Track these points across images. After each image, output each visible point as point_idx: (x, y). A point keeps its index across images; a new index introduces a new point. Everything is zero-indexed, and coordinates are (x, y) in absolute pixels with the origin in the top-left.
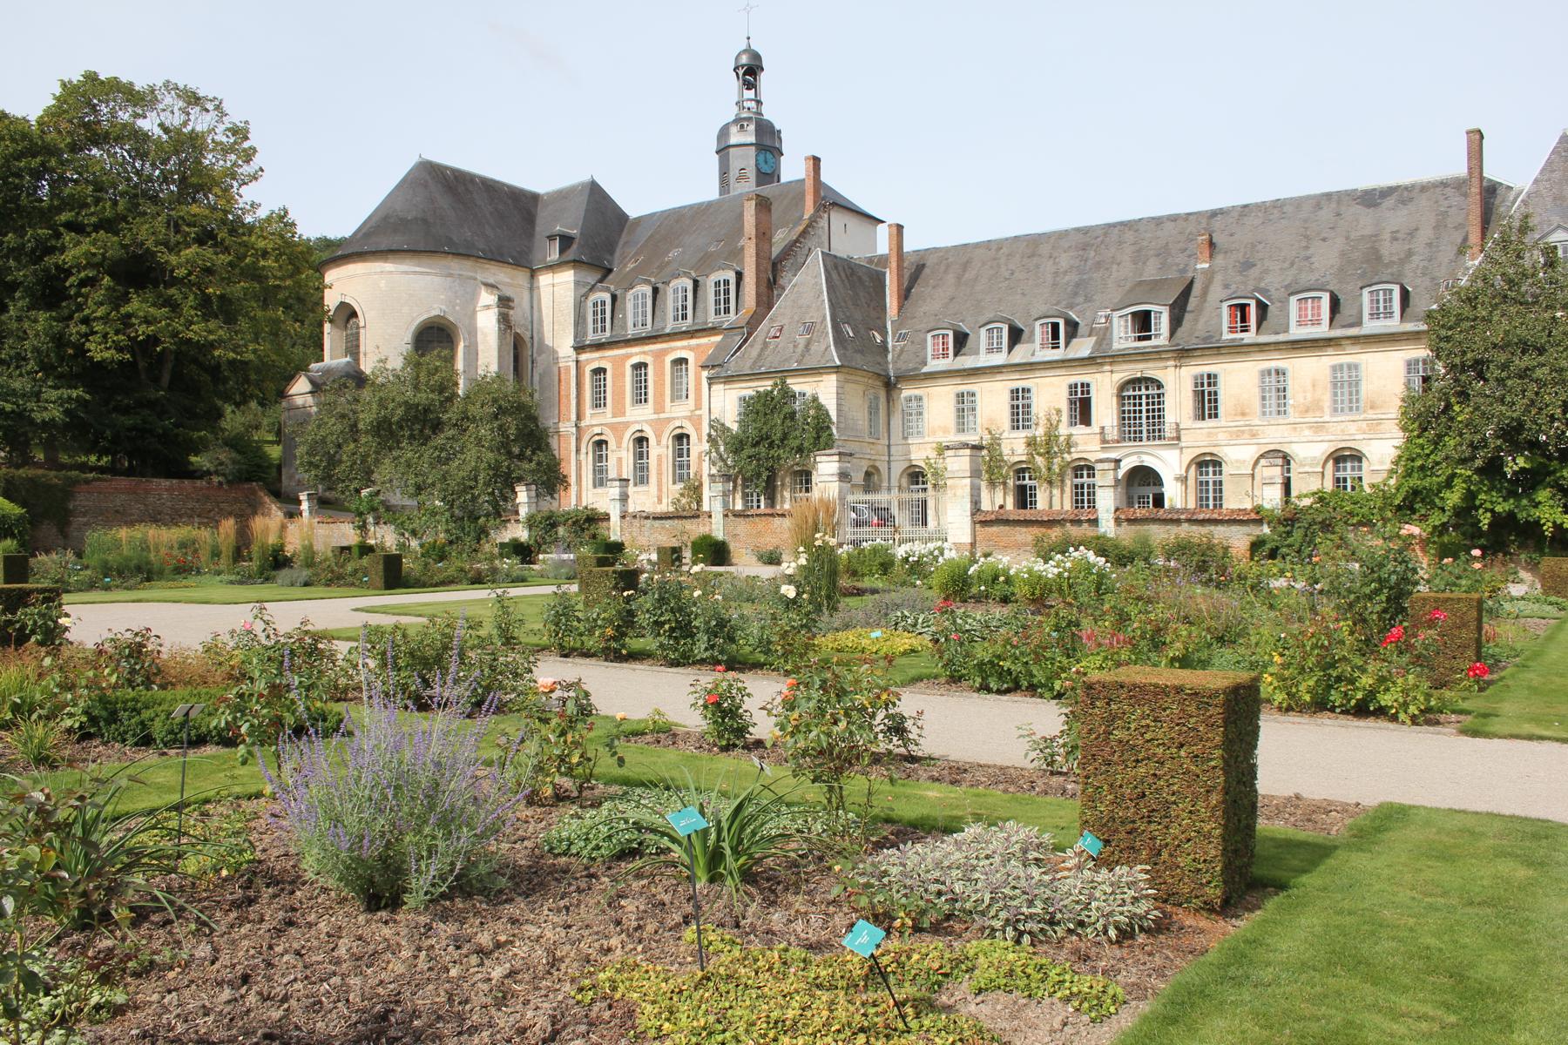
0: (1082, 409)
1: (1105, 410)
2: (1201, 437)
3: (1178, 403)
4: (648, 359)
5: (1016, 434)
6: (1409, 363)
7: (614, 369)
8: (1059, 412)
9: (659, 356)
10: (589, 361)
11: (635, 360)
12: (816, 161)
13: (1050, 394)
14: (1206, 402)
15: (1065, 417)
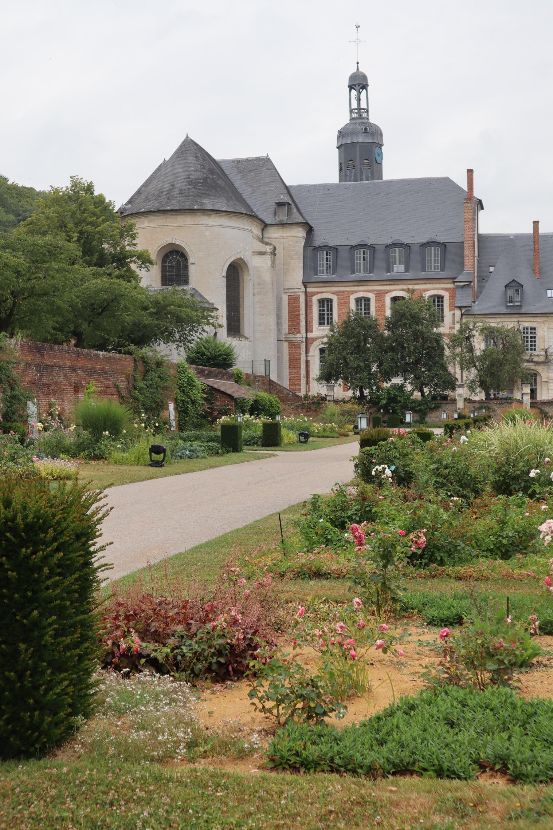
7: (339, 300)
12: (470, 172)
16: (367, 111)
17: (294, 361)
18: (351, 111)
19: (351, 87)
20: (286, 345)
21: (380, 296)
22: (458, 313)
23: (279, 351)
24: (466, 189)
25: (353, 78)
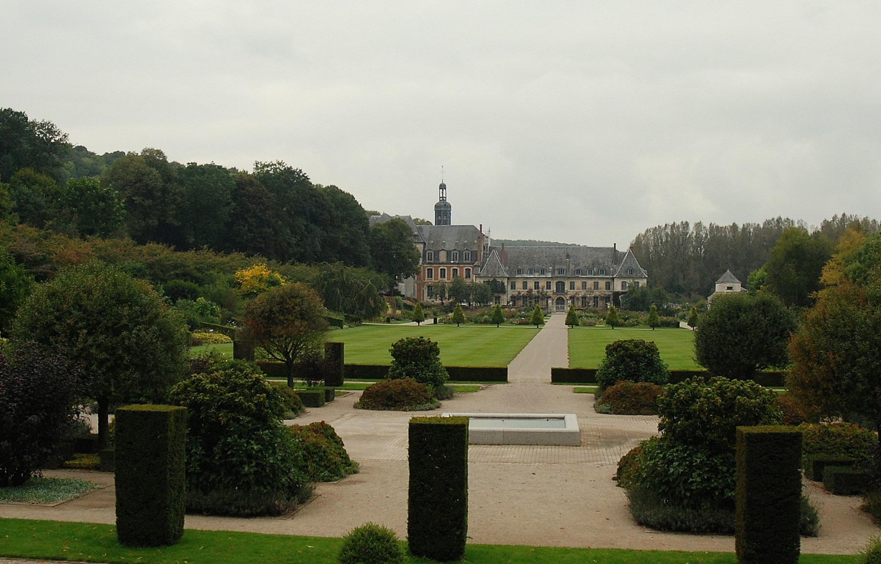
0: (549, 287)
1: (554, 287)
2: (571, 293)
3: (567, 287)
4: (445, 268)
5: (536, 290)
6: (606, 282)
8: (544, 287)
9: (449, 268)
10: (426, 267)
11: (441, 268)
13: (542, 284)
14: (572, 287)
15: (545, 288)
16: (446, 198)
17: (419, 290)
18: (440, 197)
19: (440, 189)
20: (416, 284)
21: (449, 268)
22: (474, 276)
23: (414, 286)
24: (479, 229)
25: (440, 186)
